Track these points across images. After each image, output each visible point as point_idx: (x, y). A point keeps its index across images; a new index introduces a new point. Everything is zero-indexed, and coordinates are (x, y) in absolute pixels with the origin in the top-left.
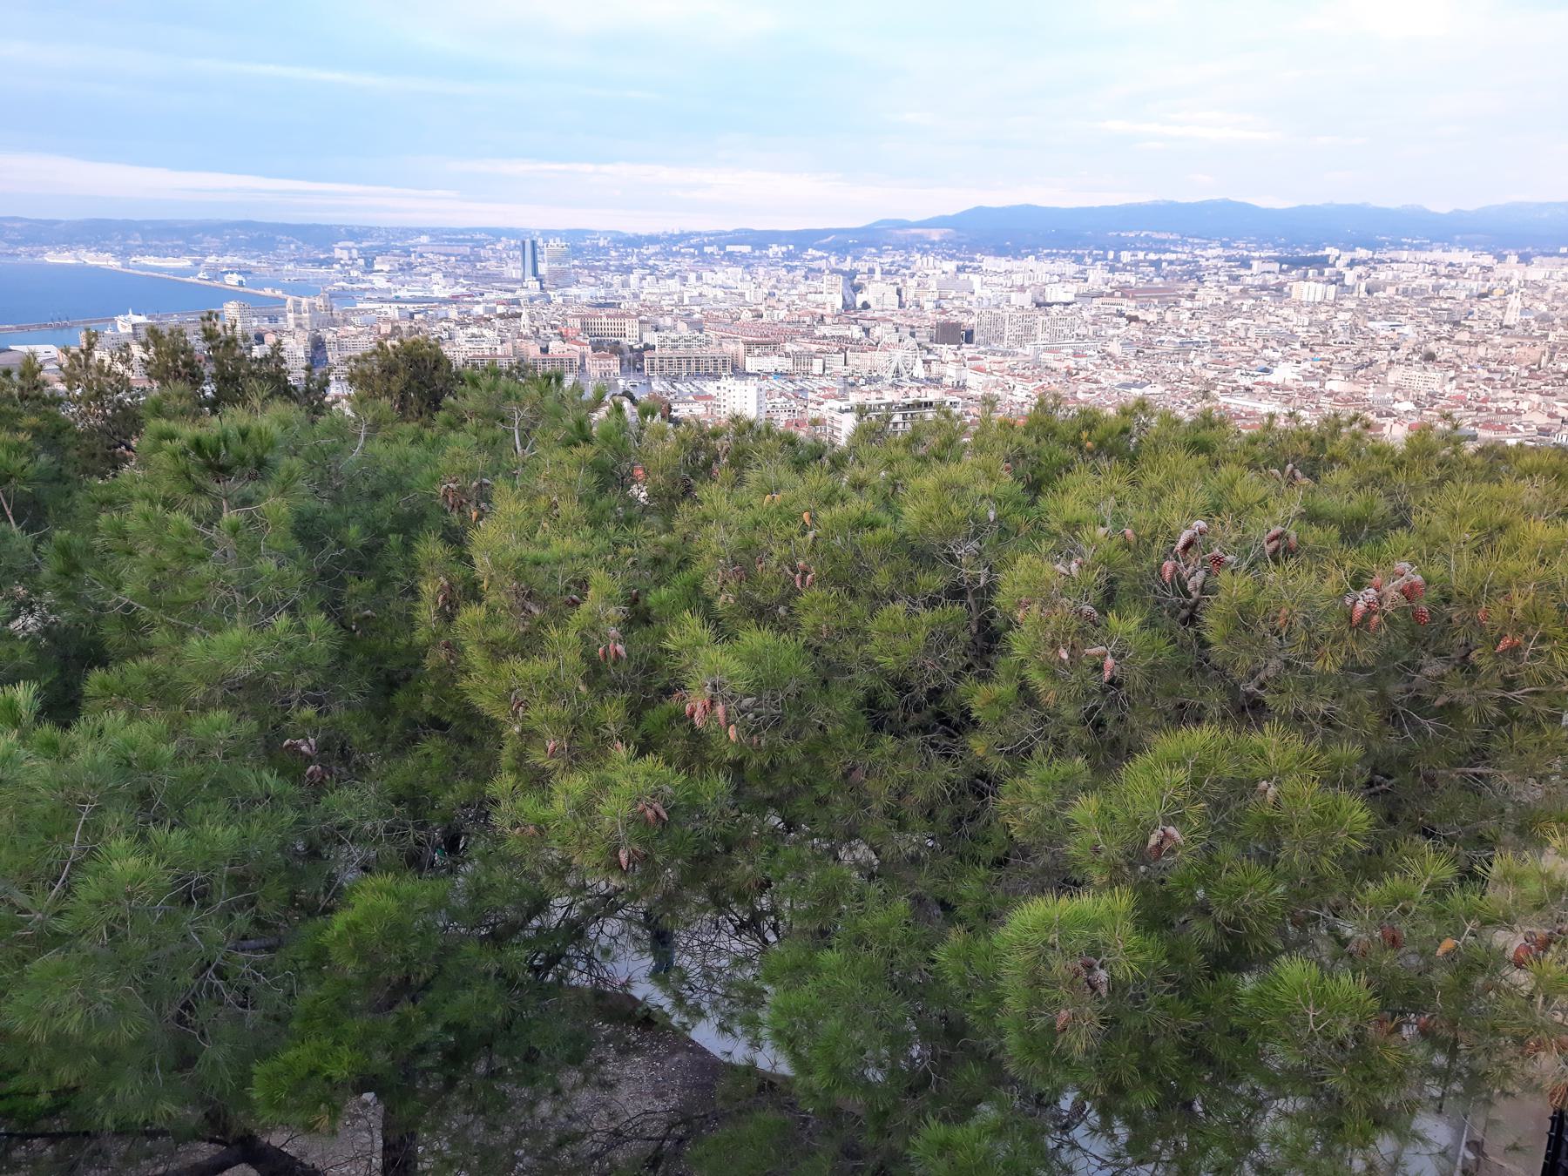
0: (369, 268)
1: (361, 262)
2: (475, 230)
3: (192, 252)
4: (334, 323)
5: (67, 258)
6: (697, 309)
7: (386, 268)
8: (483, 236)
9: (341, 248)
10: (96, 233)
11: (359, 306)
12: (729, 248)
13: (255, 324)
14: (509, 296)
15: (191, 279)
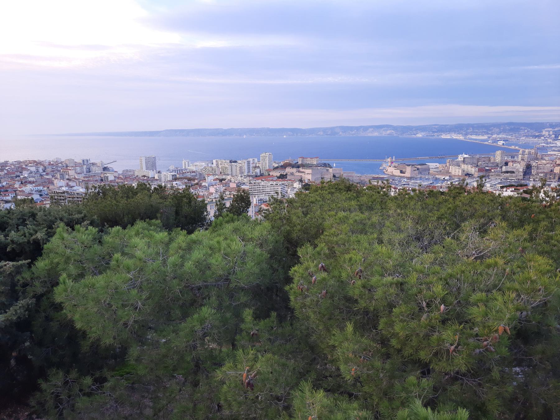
1: (553, 136)
3: (488, 134)
4: (537, 159)
5: (448, 136)
9: (546, 131)
10: (458, 128)
11: (549, 153)
13: (506, 159)
15: (486, 143)
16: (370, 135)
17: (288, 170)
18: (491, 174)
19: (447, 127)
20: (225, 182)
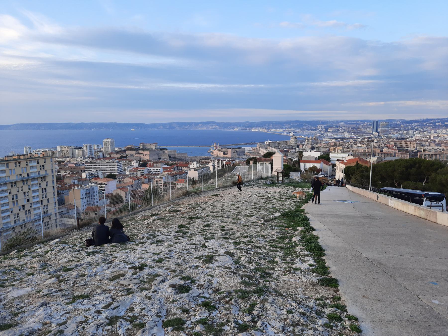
0: (326, 131)
1: (324, 129)
2: (357, 121)
3: (283, 128)
6: (436, 140)
7: (331, 131)
8: (360, 122)
11: (324, 139)
12: (446, 123)
14: (368, 137)
15: (282, 134)
16: (200, 129)
17: (128, 152)
18: (289, 153)
19: (255, 123)
20: (64, 163)
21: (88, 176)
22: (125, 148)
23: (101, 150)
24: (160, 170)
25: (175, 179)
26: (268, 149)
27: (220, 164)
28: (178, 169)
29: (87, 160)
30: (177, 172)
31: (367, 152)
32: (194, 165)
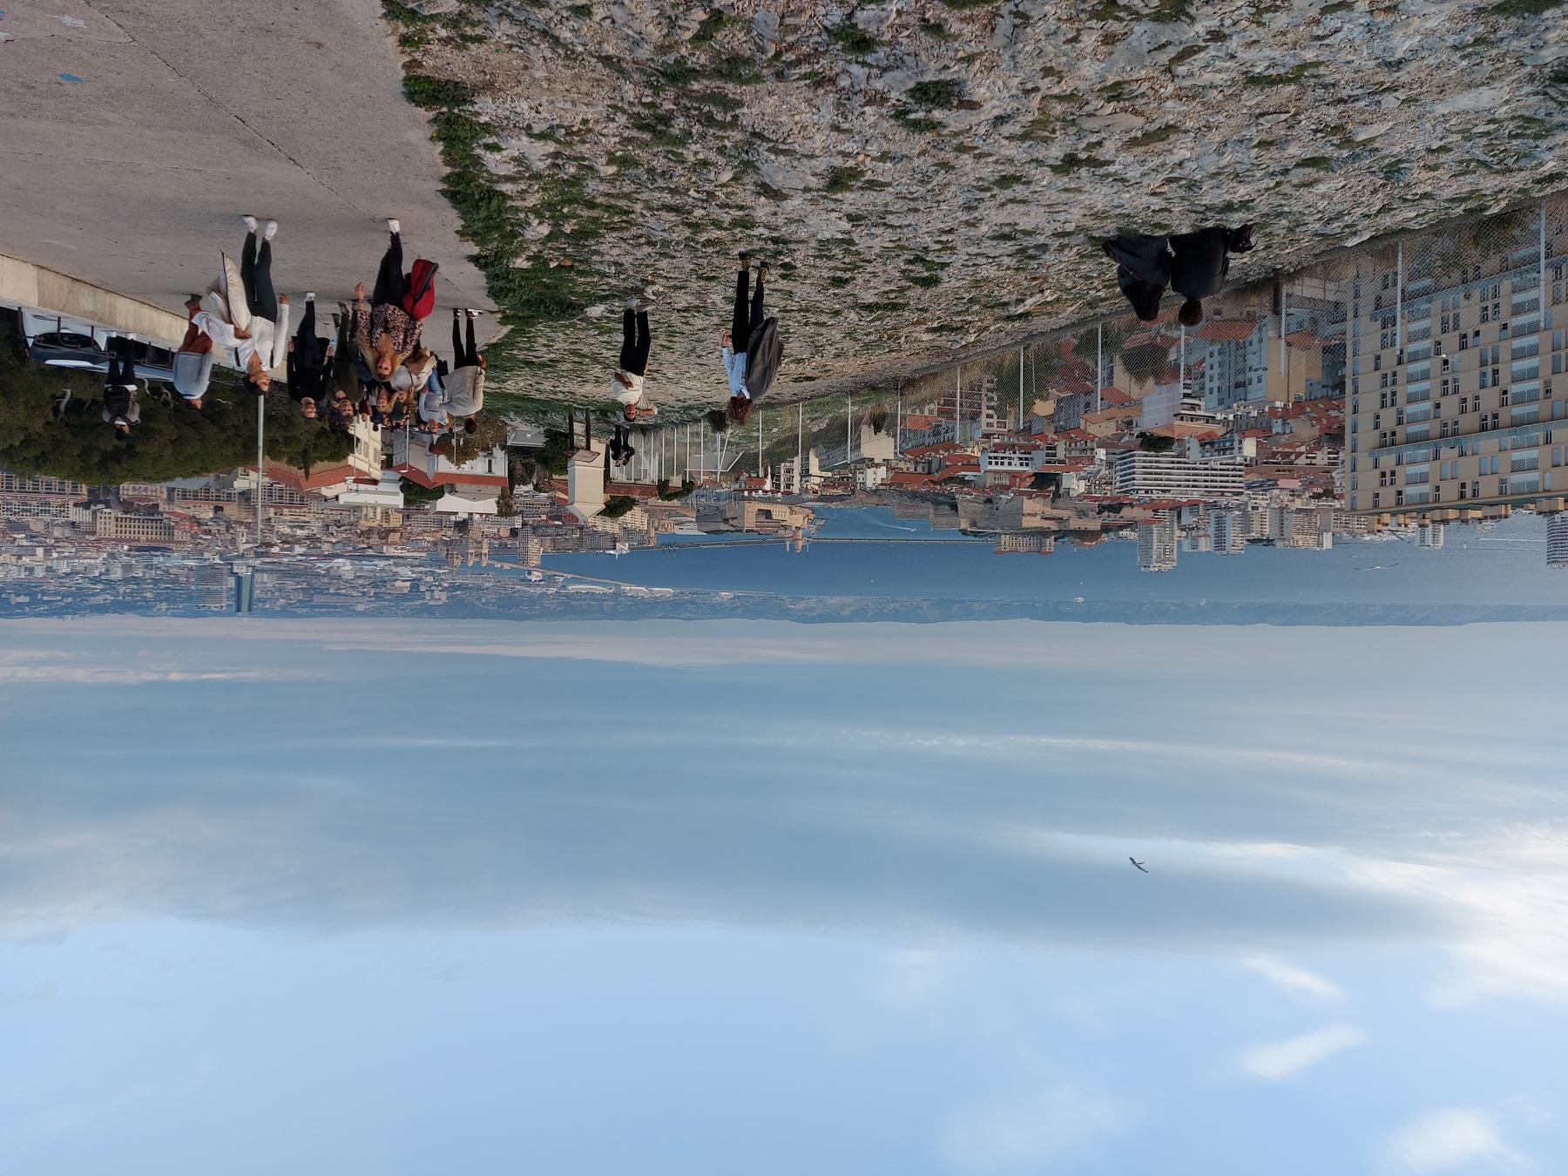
0: (416, 583)
1: (422, 588)
3: (568, 596)
6: (25, 543)
7: (398, 584)
8: (300, 611)
11: (424, 554)
14: (268, 560)
16: (848, 599)
17: (1095, 525)
20: (1315, 490)
21: (1236, 444)
22: (1105, 538)
23: (1184, 533)
24: (990, 463)
25: (940, 429)
26: (617, 526)
27: (782, 479)
28: (926, 466)
29: (1234, 501)
30: (933, 454)
31: (270, 506)
32: (874, 477)
